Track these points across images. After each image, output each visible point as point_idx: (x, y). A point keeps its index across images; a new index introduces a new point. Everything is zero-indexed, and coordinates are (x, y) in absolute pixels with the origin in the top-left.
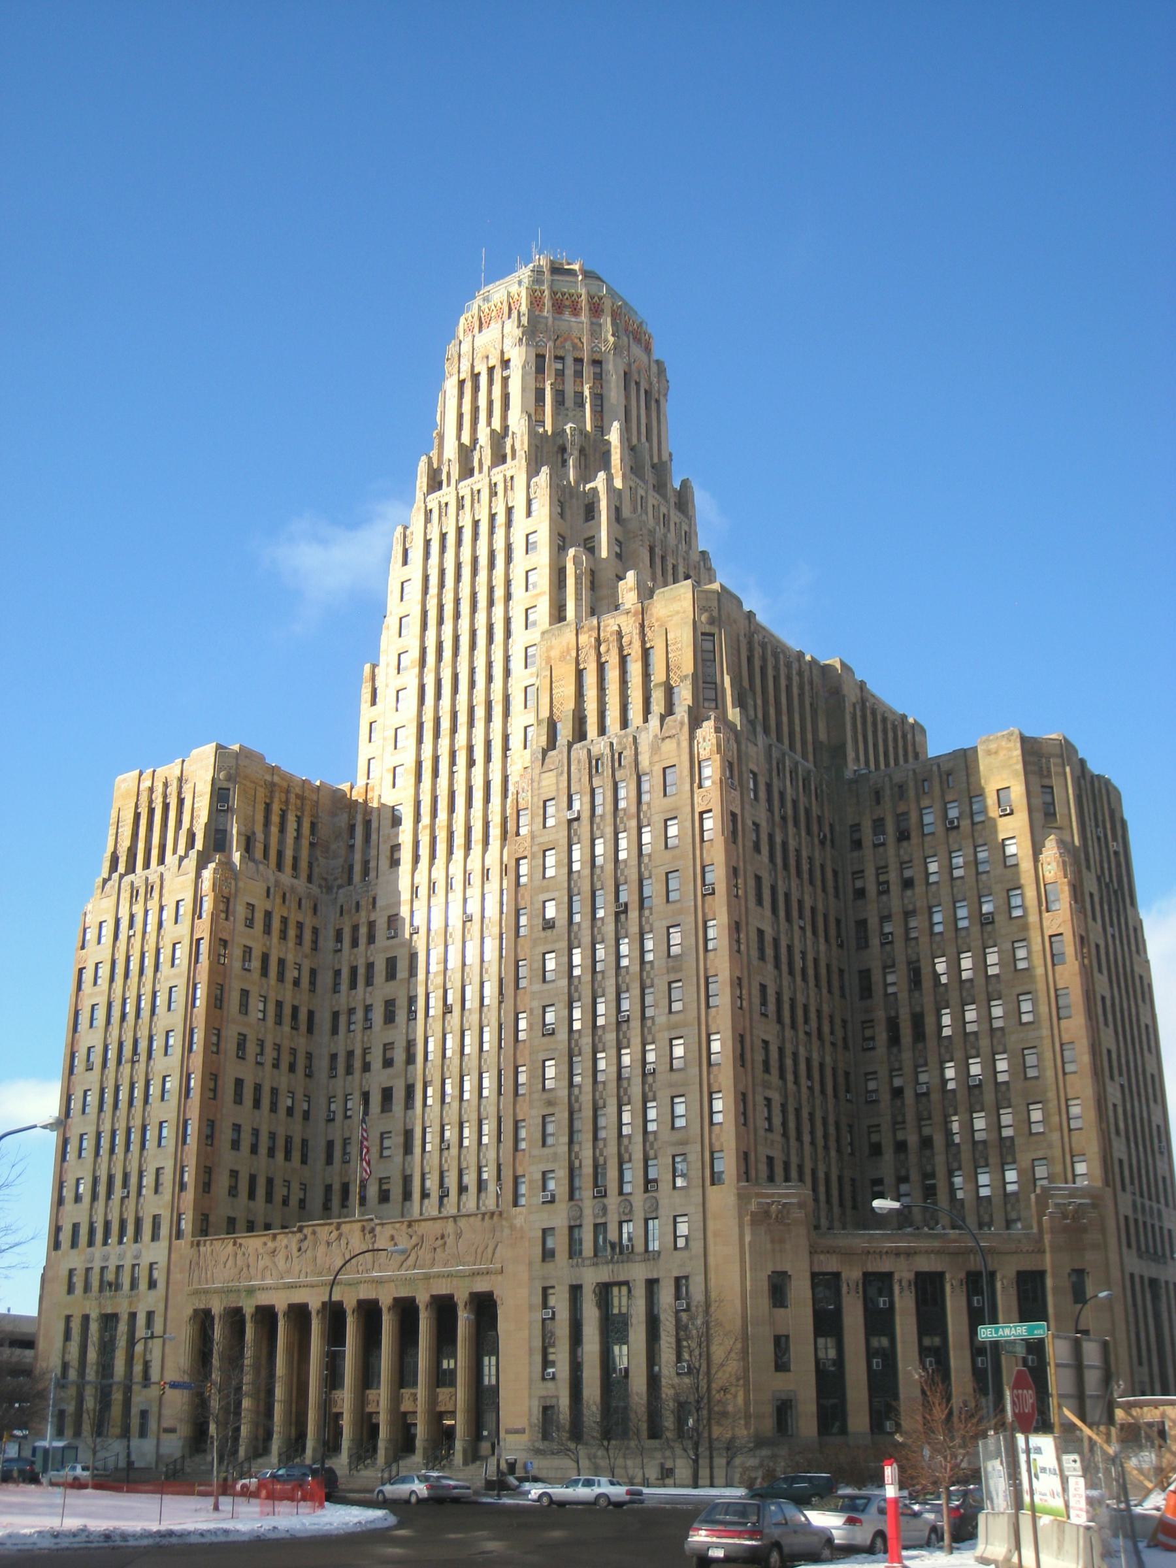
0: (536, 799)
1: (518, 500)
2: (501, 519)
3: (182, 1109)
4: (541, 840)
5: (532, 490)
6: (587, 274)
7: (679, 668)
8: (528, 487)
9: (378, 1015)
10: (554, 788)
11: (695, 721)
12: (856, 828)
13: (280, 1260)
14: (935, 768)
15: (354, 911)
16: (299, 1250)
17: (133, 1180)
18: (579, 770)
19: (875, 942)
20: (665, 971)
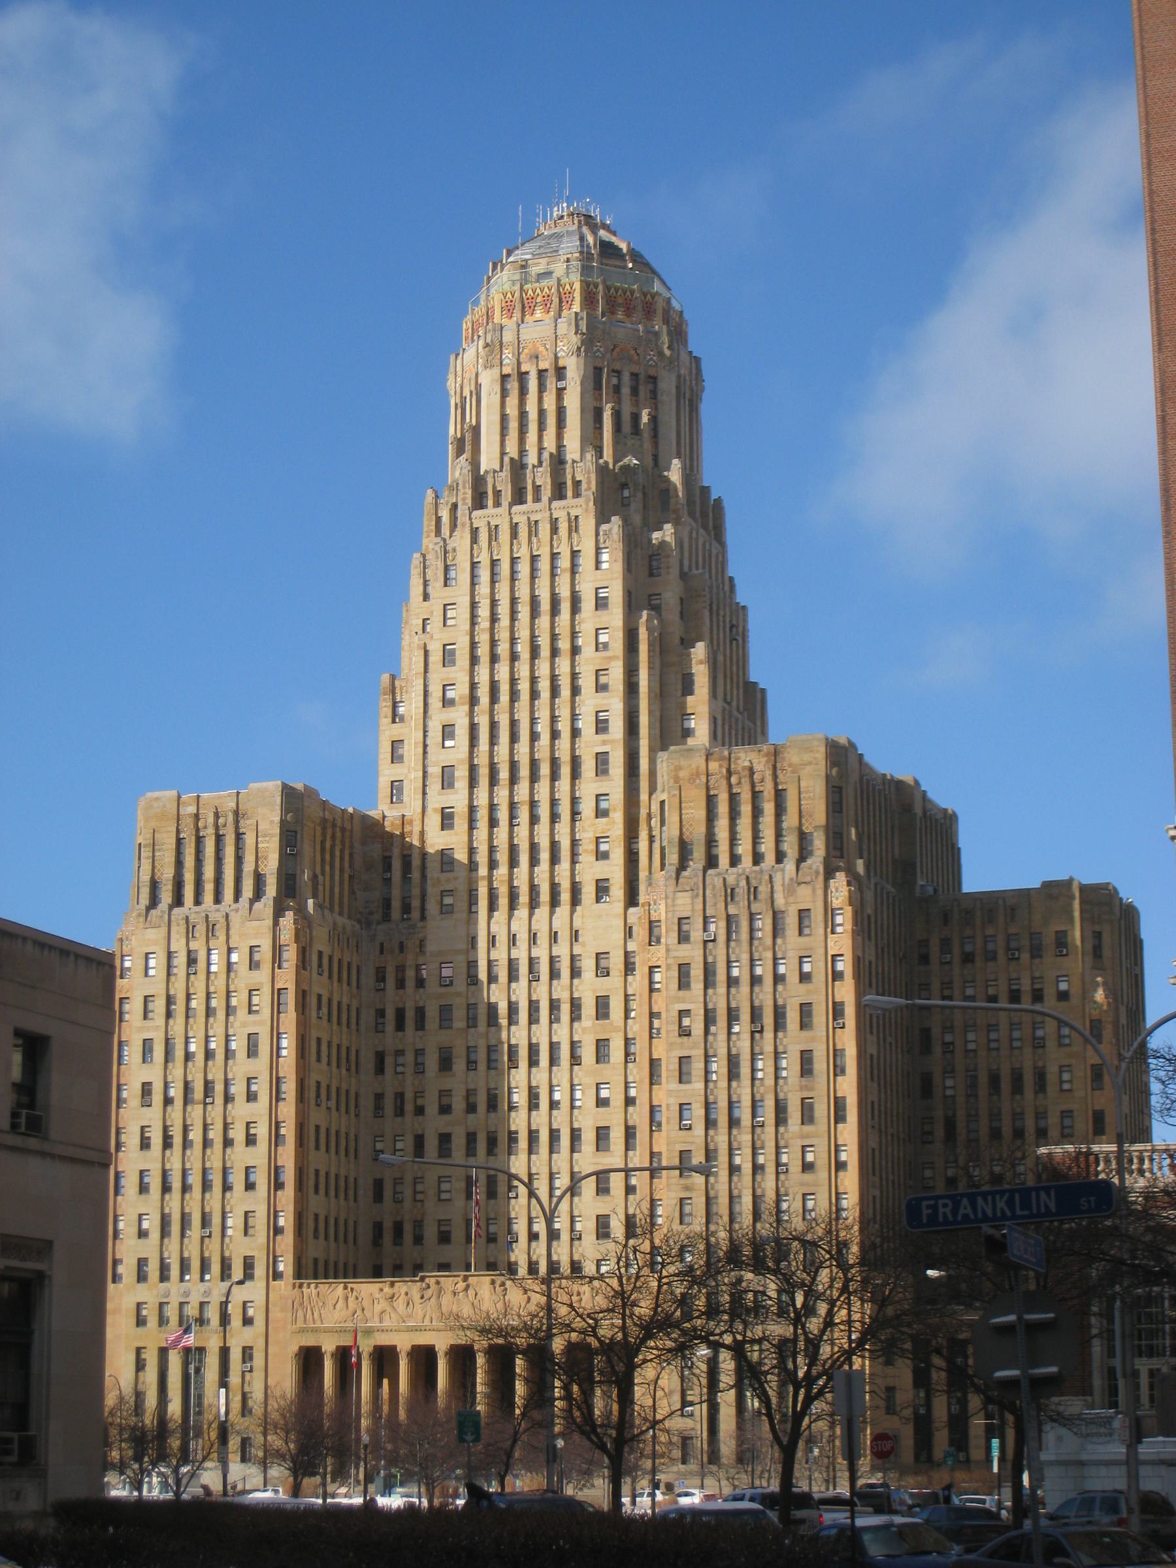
0: (670, 915)
1: (587, 546)
2: (564, 562)
3: (272, 1156)
4: (676, 954)
5: (601, 538)
6: (635, 256)
7: (811, 816)
8: (597, 534)
9: (432, 1062)
10: (689, 907)
11: (829, 874)
12: (925, 943)
13: (400, 1304)
14: (1001, 902)
15: (397, 951)
16: (422, 1297)
17: (216, 1220)
18: (714, 896)
19: (937, 1050)
20: (798, 1088)
